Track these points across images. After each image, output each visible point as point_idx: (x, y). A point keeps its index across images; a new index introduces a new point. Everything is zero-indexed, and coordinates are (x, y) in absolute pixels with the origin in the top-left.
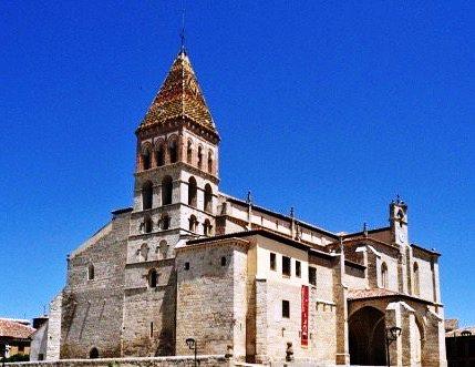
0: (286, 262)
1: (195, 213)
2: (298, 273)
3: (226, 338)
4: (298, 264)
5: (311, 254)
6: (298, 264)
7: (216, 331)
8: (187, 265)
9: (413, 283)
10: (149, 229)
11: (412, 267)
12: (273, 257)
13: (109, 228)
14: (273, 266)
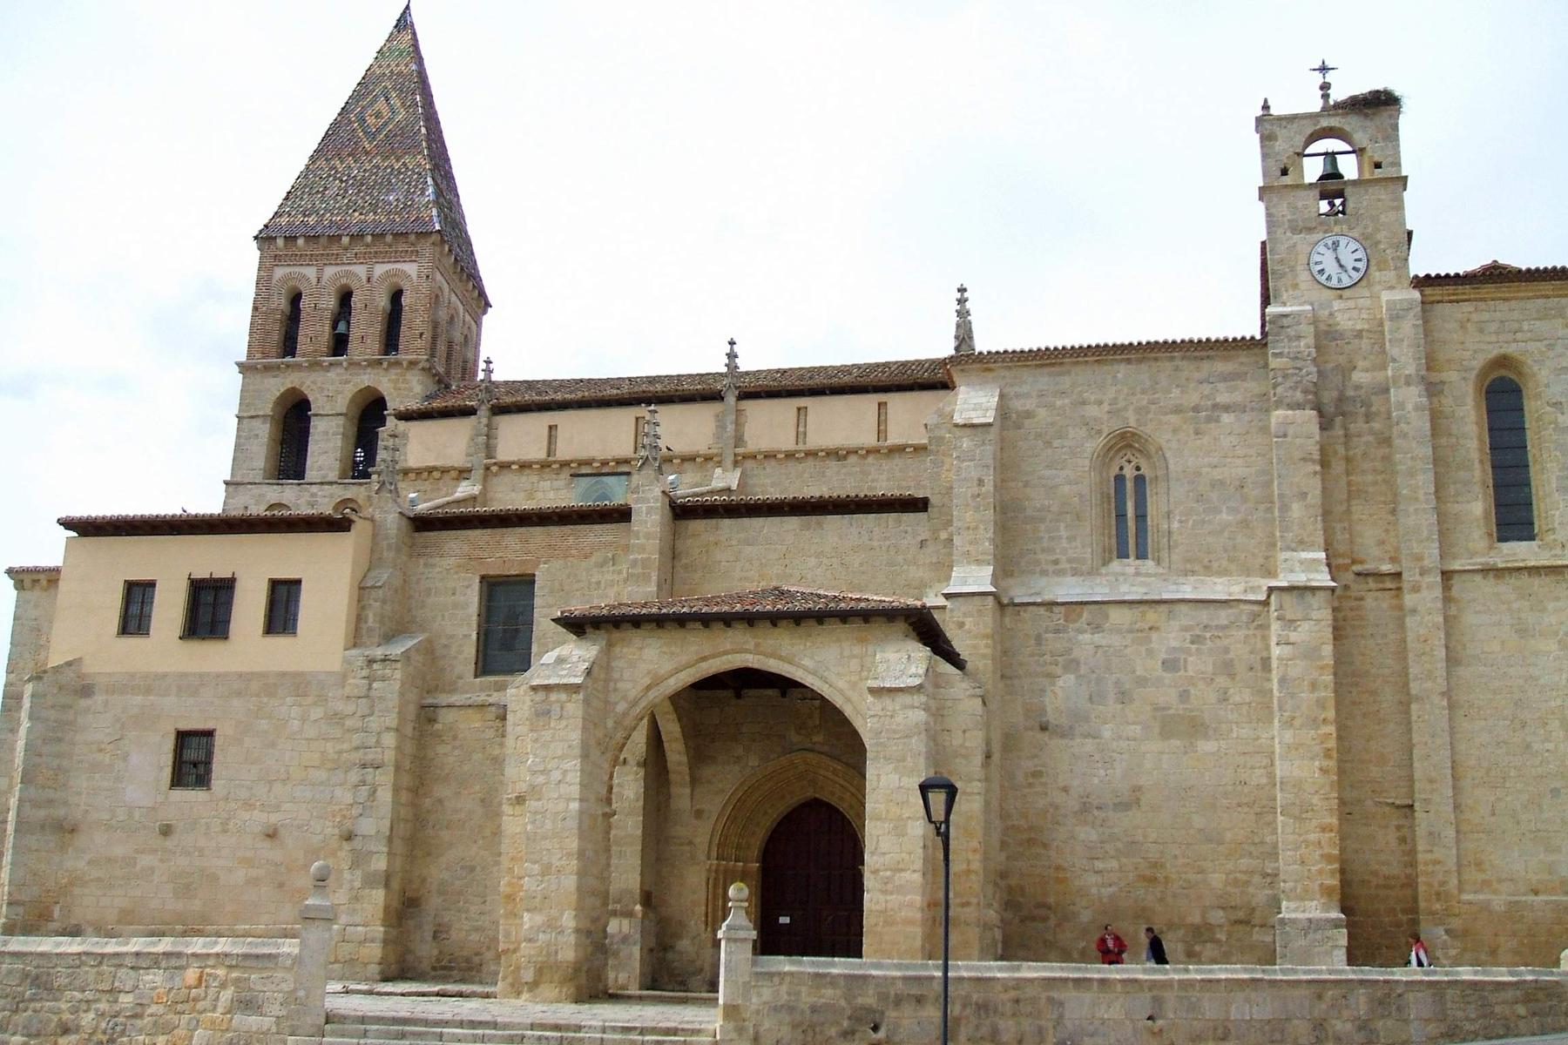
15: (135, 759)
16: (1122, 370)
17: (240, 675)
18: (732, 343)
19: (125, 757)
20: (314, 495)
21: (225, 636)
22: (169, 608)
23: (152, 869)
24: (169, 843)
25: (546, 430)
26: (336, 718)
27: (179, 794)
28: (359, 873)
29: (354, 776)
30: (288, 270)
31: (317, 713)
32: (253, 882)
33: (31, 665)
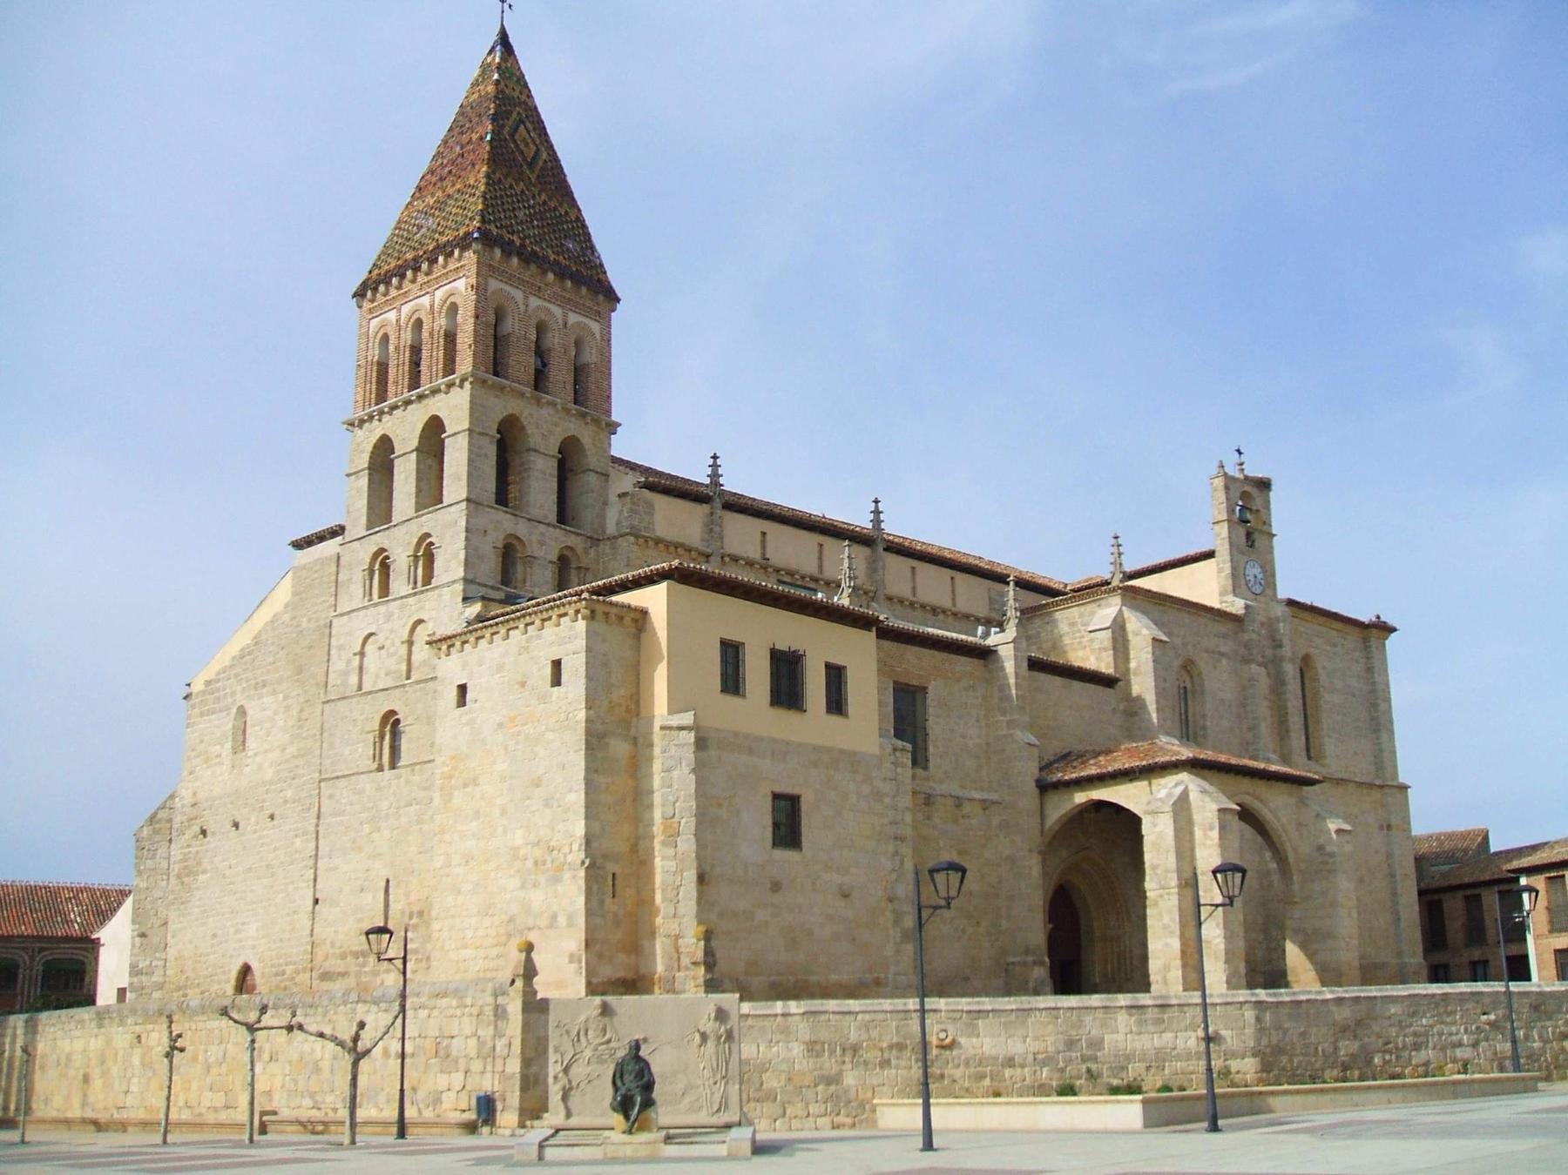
0: (786, 668)
1: (522, 529)
2: (836, 703)
3: (562, 920)
4: (835, 676)
7: (537, 898)
8: (463, 689)
10: (385, 590)
11: (1290, 670)
12: (731, 653)
14: (732, 682)
16: (1187, 618)
17: (815, 748)
18: (876, 502)
26: (878, 796)
27: (780, 854)
29: (891, 848)
30: (502, 286)
31: (866, 789)
33: (606, 703)
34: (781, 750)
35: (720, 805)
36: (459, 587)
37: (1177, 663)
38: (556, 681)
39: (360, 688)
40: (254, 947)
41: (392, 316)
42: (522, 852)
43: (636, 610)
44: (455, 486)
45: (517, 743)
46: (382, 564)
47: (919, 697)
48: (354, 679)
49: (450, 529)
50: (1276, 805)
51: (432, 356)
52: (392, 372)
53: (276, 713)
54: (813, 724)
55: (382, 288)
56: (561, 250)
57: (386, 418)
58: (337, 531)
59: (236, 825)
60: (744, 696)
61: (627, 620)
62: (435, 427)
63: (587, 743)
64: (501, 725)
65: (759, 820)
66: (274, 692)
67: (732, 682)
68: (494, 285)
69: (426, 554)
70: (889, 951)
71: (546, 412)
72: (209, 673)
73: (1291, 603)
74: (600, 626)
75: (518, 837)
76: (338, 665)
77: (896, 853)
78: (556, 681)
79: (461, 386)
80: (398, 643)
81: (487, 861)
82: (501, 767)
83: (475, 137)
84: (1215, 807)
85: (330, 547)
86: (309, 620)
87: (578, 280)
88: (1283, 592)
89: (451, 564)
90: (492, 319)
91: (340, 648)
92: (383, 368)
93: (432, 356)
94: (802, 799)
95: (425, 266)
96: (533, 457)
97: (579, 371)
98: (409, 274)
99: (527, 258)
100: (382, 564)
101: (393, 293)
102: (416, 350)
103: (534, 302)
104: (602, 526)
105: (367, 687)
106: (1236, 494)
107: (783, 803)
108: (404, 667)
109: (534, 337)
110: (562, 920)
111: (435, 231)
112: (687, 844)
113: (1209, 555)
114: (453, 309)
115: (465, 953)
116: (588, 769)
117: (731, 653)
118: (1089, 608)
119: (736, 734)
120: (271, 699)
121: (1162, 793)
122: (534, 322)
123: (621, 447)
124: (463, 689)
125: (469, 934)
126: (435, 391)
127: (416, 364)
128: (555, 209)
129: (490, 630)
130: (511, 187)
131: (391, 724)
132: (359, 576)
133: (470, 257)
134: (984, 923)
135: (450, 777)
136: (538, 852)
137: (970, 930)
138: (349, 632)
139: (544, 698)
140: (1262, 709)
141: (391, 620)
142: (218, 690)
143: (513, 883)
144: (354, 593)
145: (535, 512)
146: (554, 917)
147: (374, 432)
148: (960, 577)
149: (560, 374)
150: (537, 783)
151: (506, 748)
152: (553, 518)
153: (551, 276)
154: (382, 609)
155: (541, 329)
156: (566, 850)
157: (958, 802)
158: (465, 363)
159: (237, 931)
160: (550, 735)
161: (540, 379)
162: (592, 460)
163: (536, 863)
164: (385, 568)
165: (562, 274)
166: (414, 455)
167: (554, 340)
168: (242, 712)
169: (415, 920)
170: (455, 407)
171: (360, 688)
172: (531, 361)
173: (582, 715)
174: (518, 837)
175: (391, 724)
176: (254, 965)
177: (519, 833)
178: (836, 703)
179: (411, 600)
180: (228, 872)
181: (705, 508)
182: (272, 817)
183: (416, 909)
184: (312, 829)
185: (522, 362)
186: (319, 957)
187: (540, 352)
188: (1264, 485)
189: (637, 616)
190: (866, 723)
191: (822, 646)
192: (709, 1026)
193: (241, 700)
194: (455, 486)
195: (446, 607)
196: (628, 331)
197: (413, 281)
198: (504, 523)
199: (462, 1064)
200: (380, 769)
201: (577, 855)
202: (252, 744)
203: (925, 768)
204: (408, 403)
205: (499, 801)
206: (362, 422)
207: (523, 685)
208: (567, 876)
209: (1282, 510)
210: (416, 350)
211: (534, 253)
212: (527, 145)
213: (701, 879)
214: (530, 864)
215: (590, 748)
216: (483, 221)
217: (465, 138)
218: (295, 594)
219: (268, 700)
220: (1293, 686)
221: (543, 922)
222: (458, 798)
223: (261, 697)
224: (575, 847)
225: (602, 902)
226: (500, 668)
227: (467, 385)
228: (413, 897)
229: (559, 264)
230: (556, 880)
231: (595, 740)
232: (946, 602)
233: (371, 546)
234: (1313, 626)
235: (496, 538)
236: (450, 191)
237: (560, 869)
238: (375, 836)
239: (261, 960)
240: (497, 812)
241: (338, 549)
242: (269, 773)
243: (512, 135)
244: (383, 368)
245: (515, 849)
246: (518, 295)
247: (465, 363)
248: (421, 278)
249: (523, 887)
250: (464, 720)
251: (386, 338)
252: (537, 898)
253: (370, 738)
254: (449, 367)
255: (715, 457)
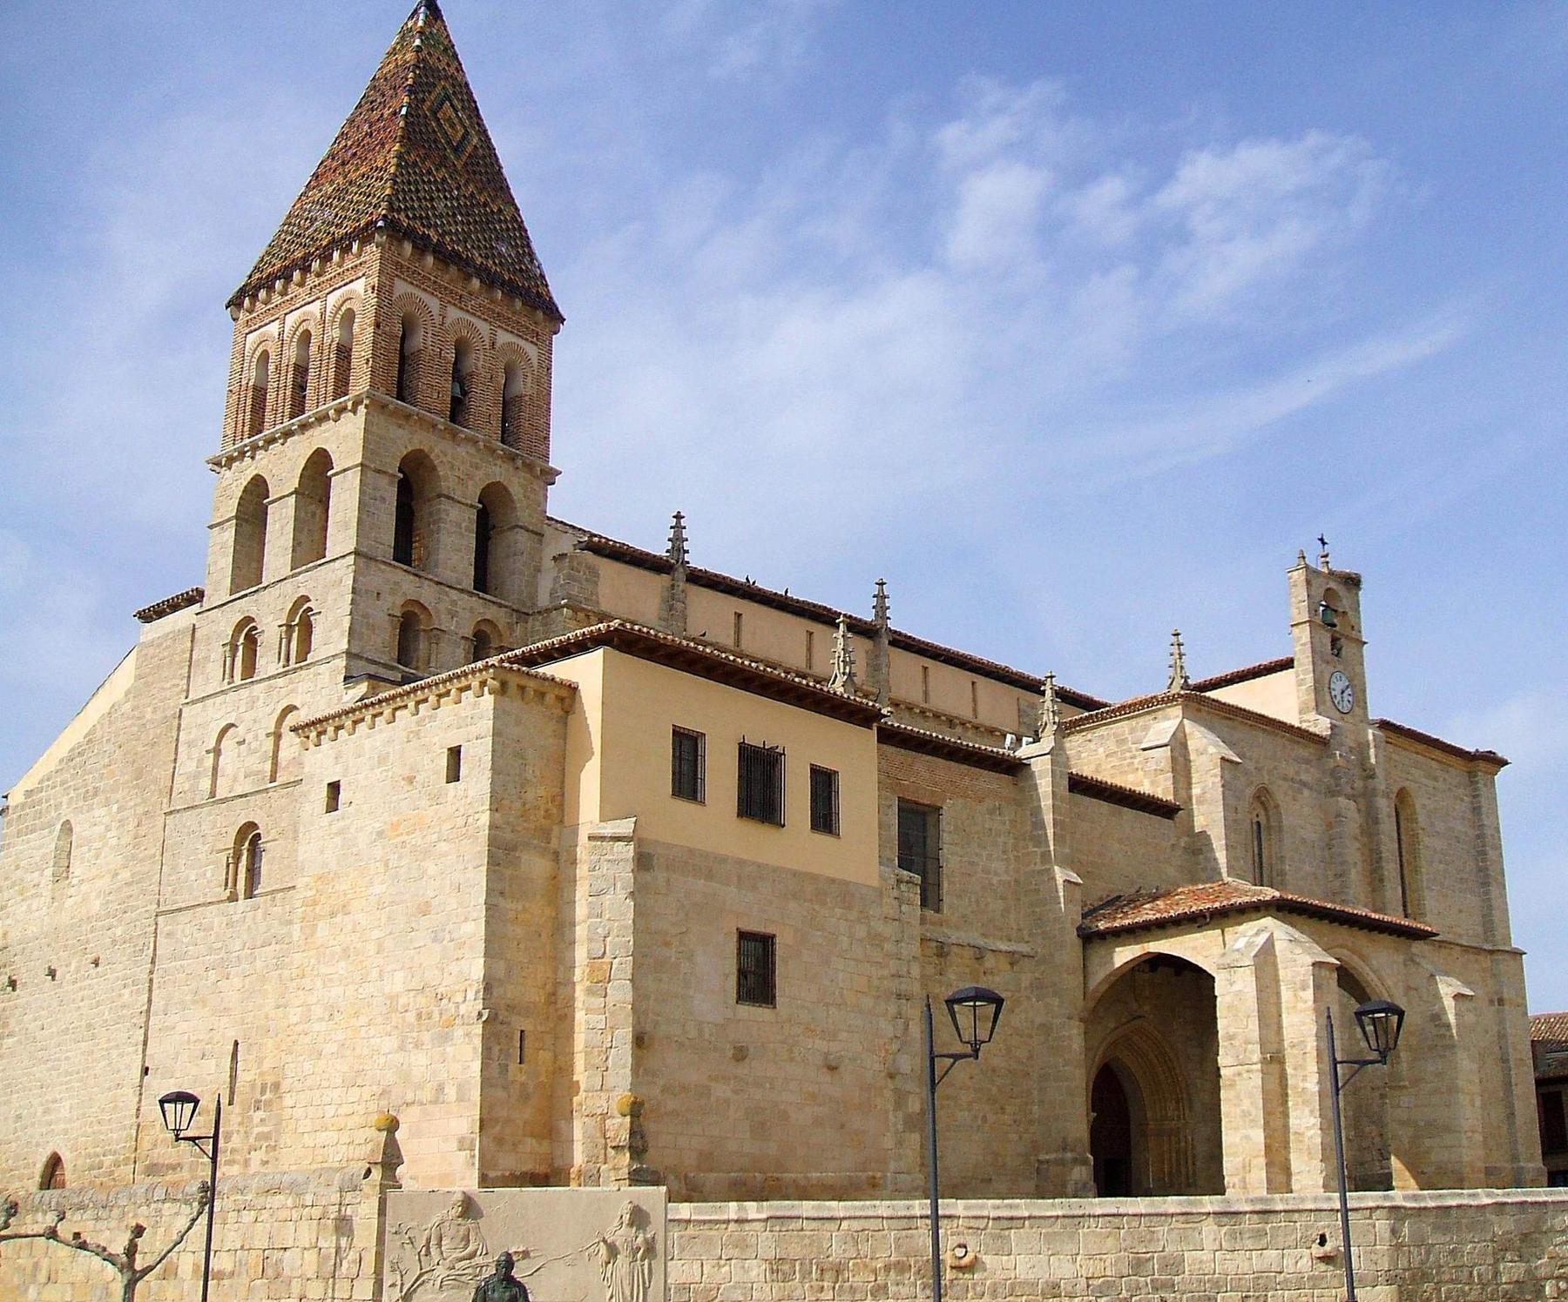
1: (427, 594)
2: (824, 818)
3: (451, 1092)
4: (823, 783)
5: (889, 737)
6: (823, 783)
8: (334, 788)
9: (1390, 869)
10: (250, 668)
11: (1385, 806)
12: (687, 746)
13: (125, 676)
14: (687, 783)
15: (700, 958)
16: (1261, 738)
17: (795, 874)
19: (690, 958)
20: (454, 603)
21: (740, 814)
22: (721, 774)
23: (727, 1102)
24: (742, 1070)
25: (732, 618)
26: (876, 939)
27: (748, 1011)
28: (900, 1114)
29: (892, 1009)
31: (861, 931)
32: (818, 1122)
33: (518, 805)
34: (749, 875)
35: (667, 944)
36: (341, 663)
37: (1250, 791)
38: (454, 775)
39: (213, 794)
40: (66, 1132)
41: (274, 328)
42: (402, 1001)
43: (561, 684)
44: (342, 535)
45: (400, 858)
46: (247, 637)
47: (931, 820)
48: (206, 784)
49: (332, 590)
50: (1383, 967)
51: (321, 377)
52: (271, 396)
53: (108, 829)
54: (793, 842)
55: (262, 294)
56: (491, 253)
57: (260, 454)
58: (194, 597)
59: (52, 973)
60: (702, 803)
61: (550, 698)
62: (320, 464)
63: (491, 856)
64: (380, 834)
65: (718, 966)
66: (107, 804)
67: (687, 783)
68: (401, 288)
69: (301, 623)
70: (888, 1142)
71: (462, 450)
72: (29, 782)
73: (1385, 725)
74: (514, 704)
75: (397, 982)
76: (187, 765)
77: (899, 1015)
78: (454, 775)
79: (354, 411)
80: (262, 736)
81: (357, 1015)
82: (378, 889)
83: (387, 113)
84: (1310, 960)
85: (186, 616)
86: (155, 711)
87: (512, 290)
88: (1377, 710)
89: (331, 636)
90: (398, 330)
91: (190, 744)
92: (260, 394)
93: (321, 377)
94: (778, 940)
95: (315, 265)
96: (445, 505)
97: (509, 405)
98: (297, 275)
99: (446, 258)
100: (247, 637)
101: (276, 299)
102: (301, 370)
103: (454, 313)
104: (533, 597)
105: (220, 795)
106: (1319, 592)
107: (752, 945)
108: (268, 766)
109: (452, 357)
110: (451, 1092)
111: (331, 224)
112: (621, 992)
113: (1287, 664)
114: (350, 316)
115: (323, 1137)
116: (490, 892)
117: (687, 746)
118: (1141, 721)
119: (691, 851)
120: (103, 811)
121: (1241, 943)
122: (452, 338)
123: (561, 503)
124: (334, 788)
125: (331, 1111)
126: (322, 418)
127: (300, 387)
128: (485, 205)
129: (372, 711)
130: (429, 172)
131: (250, 839)
132: (218, 653)
133: (372, 253)
134: (1009, 1109)
135: (315, 903)
136: (422, 1001)
137: (991, 1118)
138: (203, 722)
139: (436, 799)
140: (1353, 853)
141: (254, 709)
142: (40, 802)
143: (390, 1043)
144: (211, 675)
145: (447, 575)
146: (440, 1089)
147: (244, 472)
148: (982, 681)
149: (484, 403)
150: (425, 909)
151: (386, 865)
152: (469, 583)
153: (476, 283)
154: (244, 693)
155: (461, 348)
156: (459, 998)
157: (980, 954)
158: (360, 382)
159: (45, 1112)
160: (443, 846)
161: (458, 410)
162: (523, 515)
163: (419, 1016)
164: (251, 641)
165: (491, 281)
166: (292, 499)
167: (477, 362)
168: (67, 828)
169: (268, 1096)
170: (345, 438)
171: (213, 794)
172: (448, 386)
173: (485, 819)
174: (397, 982)
175: (250, 839)
176: (66, 1157)
177: (399, 976)
178: (824, 818)
179: (280, 681)
180: (39, 1034)
181: (665, 579)
182: (96, 963)
183: (270, 1080)
184: (145, 976)
185: (435, 387)
186: (146, 1144)
187: (459, 375)
188: (1353, 582)
189: (564, 693)
190: (862, 846)
191: (805, 742)
192: (623, 1236)
193: (66, 813)
194: (342, 535)
195: (323, 687)
196: (571, 357)
197: (301, 284)
198: (404, 585)
199: (296, 1288)
200: (233, 898)
201: (473, 1004)
202: (77, 869)
203: (938, 911)
204: (288, 434)
205: (376, 934)
206: (231, 460)
207: (411, 780)
208: (459, 1032)
209: (1373, 614)
210: (301, 370)
211: (458, 254)
212: (453, 126)
213: (640, 1041)
214: (411, 1017)
215: (494, 863)
216: (391, 208)
217: (375, 115)
218: (138, 677)
219: (99, 812)
220: (1388, 826)
221: (426, 1094)
222: (323, 931)
223: (91, 809)
224: (471, 995)
225: (504, 1069)
226: (382, 760)
227: (362, 409)
228: (267, 1065)
229: (487, 268)
230: (445, 1038)
231: (502, 853)
232: (965, 712)
233: (234, 615)
234: (1409, 757)
235: (393, 604)
236: (352, 176)
237: (450, 1024)
238: (223, 984)
239: (74, 1149)
240: (371, 948)
241: (194, 620)
242: (96, 905)
243: (435, 114)
244: (260, 394)
245: (393, 998)
246: (434, 304)
247: (360, 382)
248: (311, 280)
249: (402, 1048)
250: (334, 829)
251: (265, 356)
252: (419, 1061)
253: (223, 857)
254: (342, 386)
255: (678, 517)
